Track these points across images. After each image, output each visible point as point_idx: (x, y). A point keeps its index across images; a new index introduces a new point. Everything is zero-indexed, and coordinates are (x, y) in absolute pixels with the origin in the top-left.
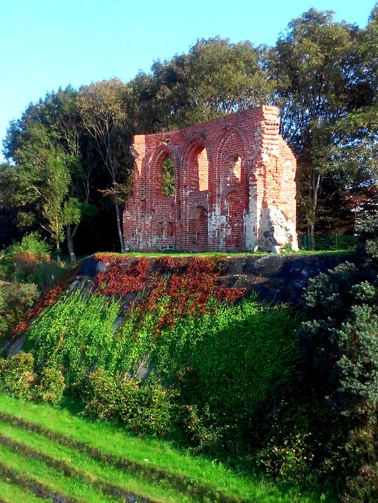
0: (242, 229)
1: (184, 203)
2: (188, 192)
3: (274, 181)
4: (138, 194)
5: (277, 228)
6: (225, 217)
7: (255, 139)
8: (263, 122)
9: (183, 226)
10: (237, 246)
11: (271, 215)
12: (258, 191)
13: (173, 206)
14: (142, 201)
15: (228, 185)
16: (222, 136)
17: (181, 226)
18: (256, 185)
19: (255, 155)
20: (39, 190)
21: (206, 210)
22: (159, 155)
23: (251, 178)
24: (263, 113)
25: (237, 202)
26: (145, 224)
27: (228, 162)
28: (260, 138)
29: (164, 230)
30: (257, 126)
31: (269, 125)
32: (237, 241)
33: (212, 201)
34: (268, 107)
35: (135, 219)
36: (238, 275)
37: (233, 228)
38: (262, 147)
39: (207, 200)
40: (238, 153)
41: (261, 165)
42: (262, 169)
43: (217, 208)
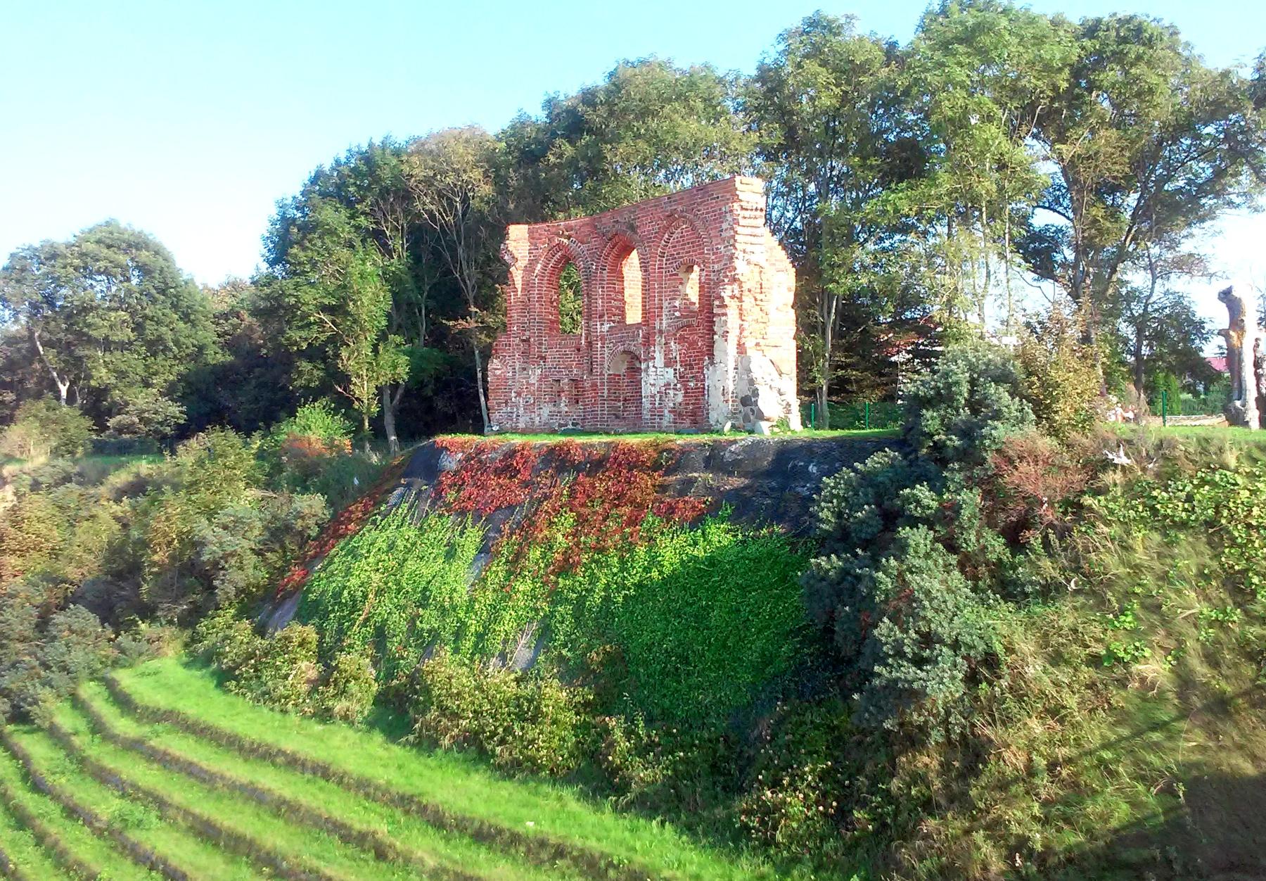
0: (702, 391)
1: (599, 345)
2: (606, 327)
3: (758, 308)
6: (671, 371)
7: (724, 234)
8: (736, 206)
10: (695, 422)
12: (729, 325)
13: (579, 350)
16: (666, 228)
17: (594, 385)
18: (725, 315)
19: (723, 263)
20: (333, 322)
21: (638, 358)
23: (717, 303)
24: (736, 189)
25: (692, 344)
26: (528, 383)
27: (677, 275)
29: (562, 394)
30: (726, 212)
32: (694, 414)
33: (648, 341)
34: (745, 180)
35: (510, 374)
36: (696, 475)
37: (686, 389)
38: (736, 249)
39: (640, 340)
41: (734, 280)
42: (736, 286)
43: (657, 355)
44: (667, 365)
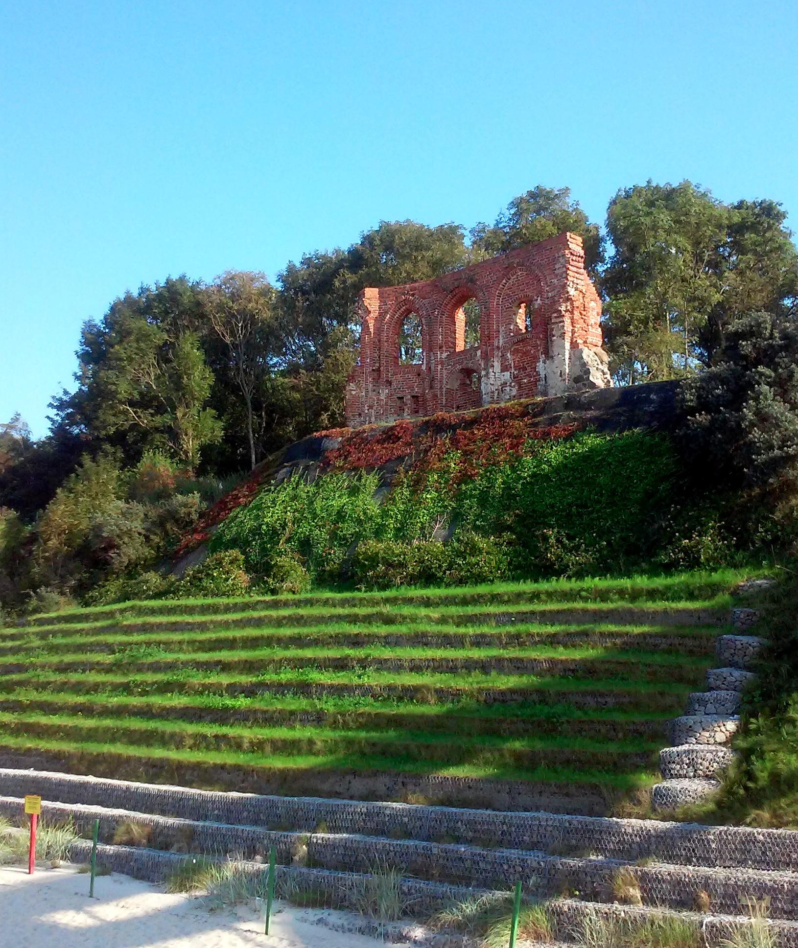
1: (440, 367)
2: (445, 355)
3: (582, 320)
5: (593, 370)
11: (584, 356)
12: (565, 328)
13: (419, 375)
14: (373, 370)
15: (512, 334)
18: (564, 322)
20: (135, 413)
24: (568, 240)
26: (378, 399)
28: (564, 269)
31: (574, 255)
34: (573, 236)
35: (364, 394)
38: (567, 279)
41: (568, 299)
42: (568, 304)
44: (502, 371)
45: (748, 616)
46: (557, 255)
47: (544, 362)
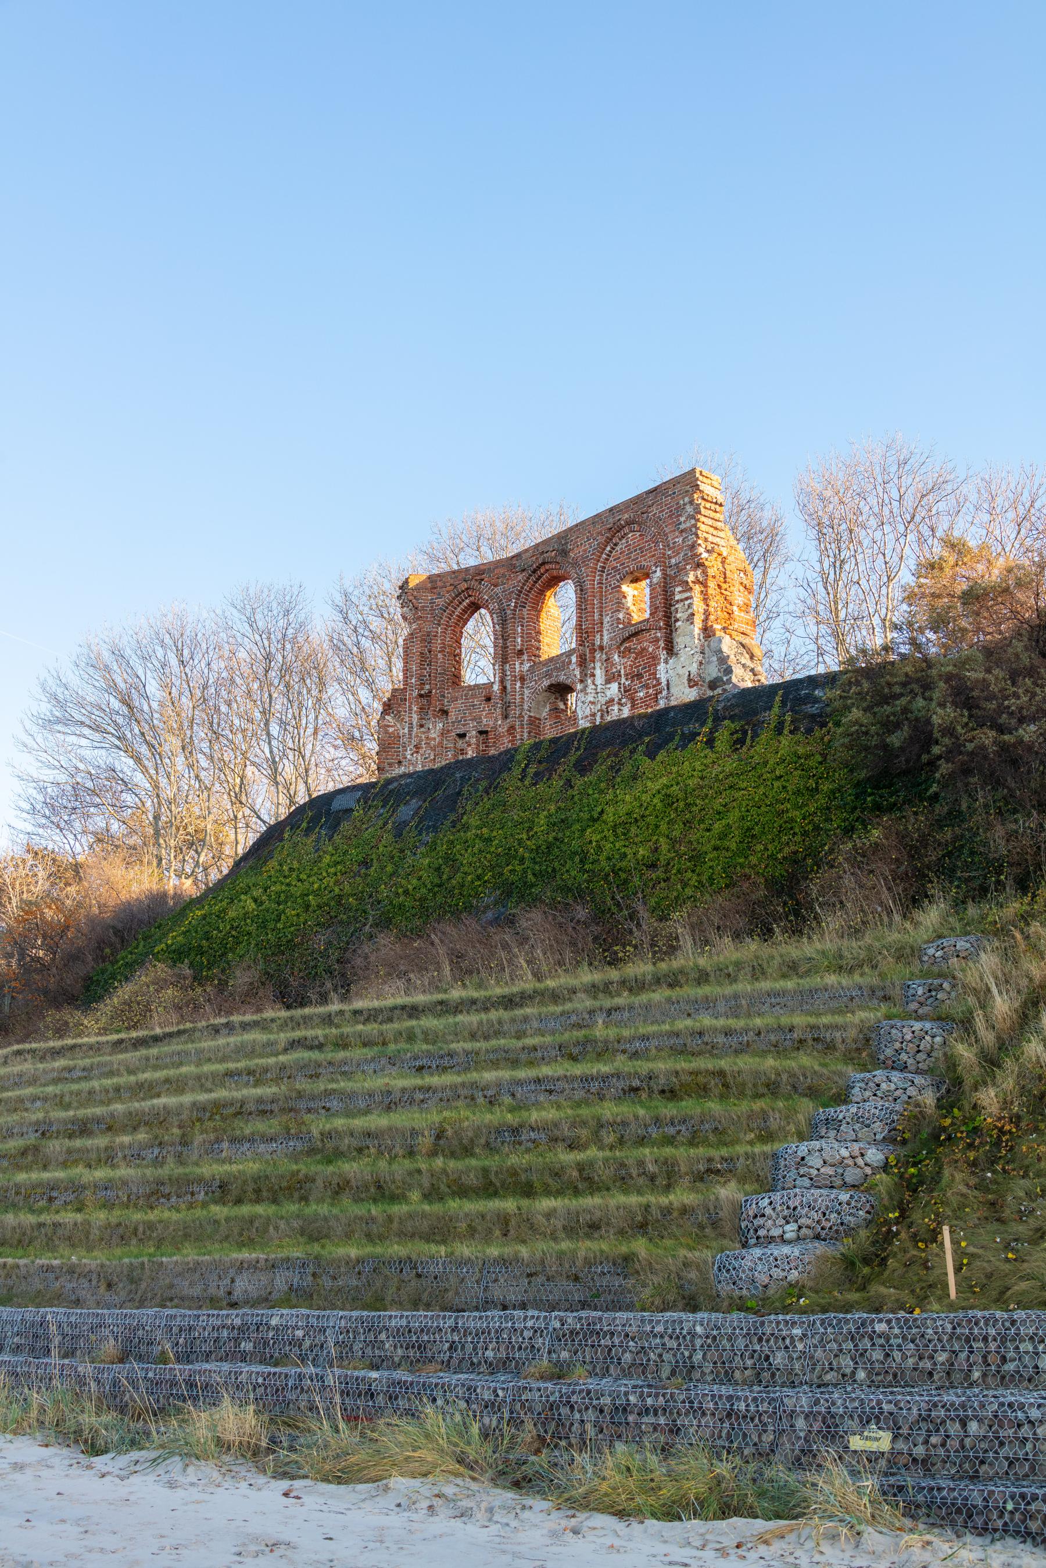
1: (518, 684)
2: (527, 666)
4: (413, 681)
9: (515, 729)
14: (421, 696)
15: (621, 626)
22: (459, 609)
23: (679, 589)
24: (697, 479)
28: (693, 522)
30: (684, 505)
35: (406, 731)
37: (633, 700)
38: (697, 537)
40: (643, 563)
41: (699, 565)
42: (699, 572)
44: (608, 681)
45: (930, 991)
46: (682, 502)
47: (666, 662)
